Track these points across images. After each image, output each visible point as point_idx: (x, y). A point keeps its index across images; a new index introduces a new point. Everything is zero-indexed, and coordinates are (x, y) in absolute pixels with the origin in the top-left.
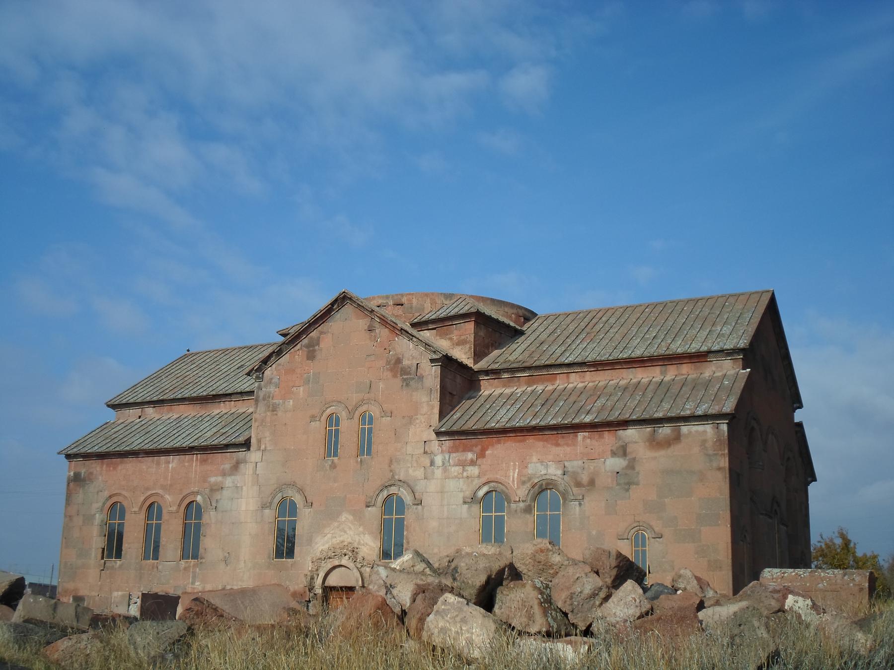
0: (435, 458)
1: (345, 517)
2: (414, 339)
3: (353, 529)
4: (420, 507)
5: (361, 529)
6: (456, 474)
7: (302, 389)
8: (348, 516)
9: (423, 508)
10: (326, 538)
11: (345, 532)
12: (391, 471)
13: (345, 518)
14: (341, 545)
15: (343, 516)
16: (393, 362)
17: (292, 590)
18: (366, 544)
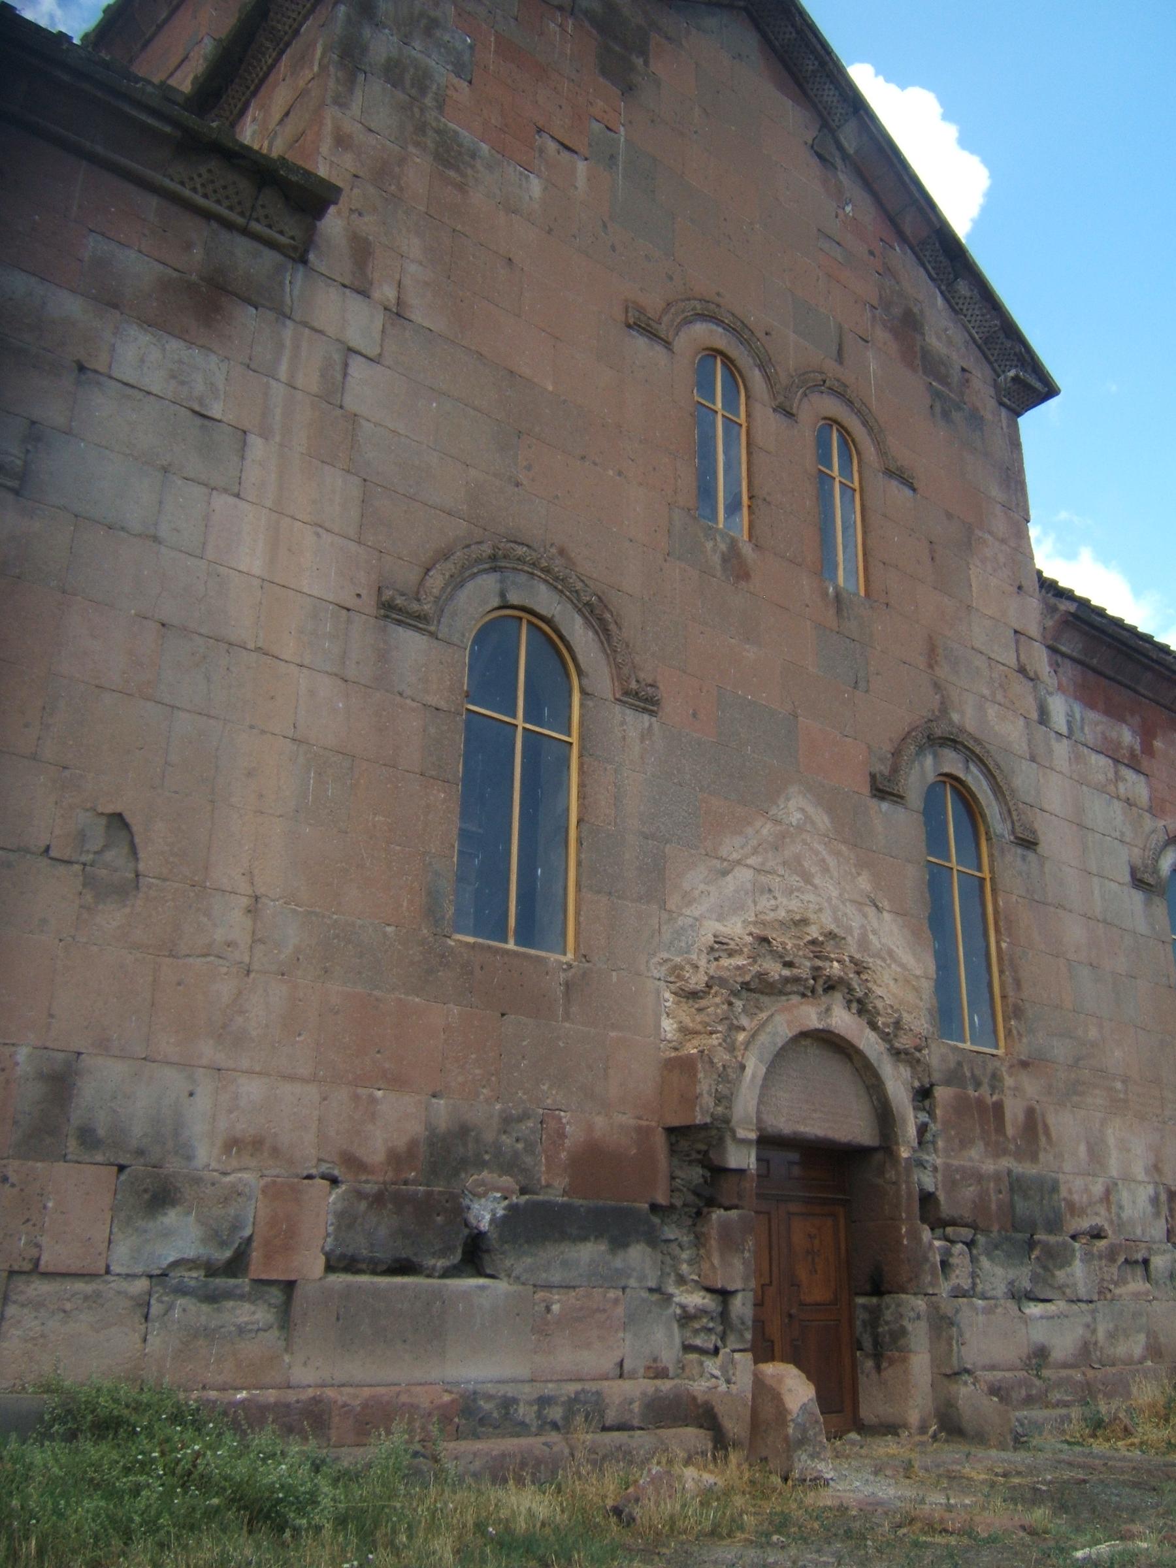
0: (1050, 700)
1: (802, 810)
2: (963, 287)
3: (835, 874)
4: (1031, 856)
5: (864, 882)
6: (1101, 777)
7: (581, 166)
8: (811, 810)
9: (1042, 865)
10: (730, 884)
11: (807, 878)
12: (937, 686)
13: (799, 815)
14: (794, 931)
15: (792, 804)
16: (897, 311)
17: (574, 1132)
18: (891, 953)
